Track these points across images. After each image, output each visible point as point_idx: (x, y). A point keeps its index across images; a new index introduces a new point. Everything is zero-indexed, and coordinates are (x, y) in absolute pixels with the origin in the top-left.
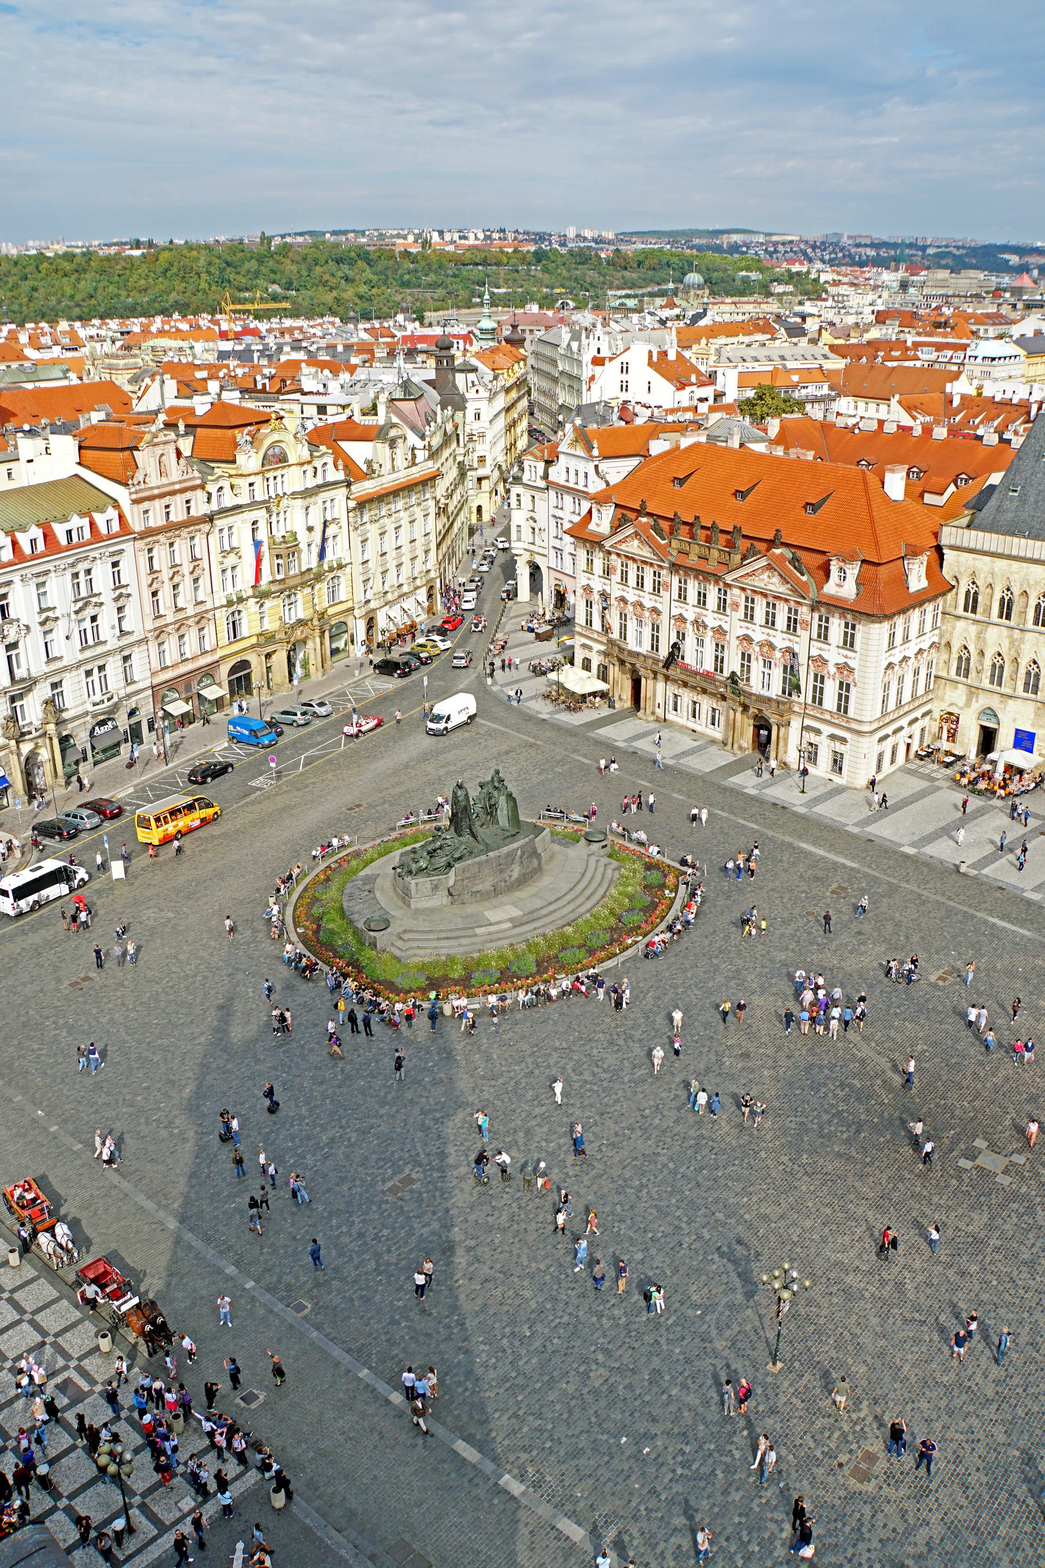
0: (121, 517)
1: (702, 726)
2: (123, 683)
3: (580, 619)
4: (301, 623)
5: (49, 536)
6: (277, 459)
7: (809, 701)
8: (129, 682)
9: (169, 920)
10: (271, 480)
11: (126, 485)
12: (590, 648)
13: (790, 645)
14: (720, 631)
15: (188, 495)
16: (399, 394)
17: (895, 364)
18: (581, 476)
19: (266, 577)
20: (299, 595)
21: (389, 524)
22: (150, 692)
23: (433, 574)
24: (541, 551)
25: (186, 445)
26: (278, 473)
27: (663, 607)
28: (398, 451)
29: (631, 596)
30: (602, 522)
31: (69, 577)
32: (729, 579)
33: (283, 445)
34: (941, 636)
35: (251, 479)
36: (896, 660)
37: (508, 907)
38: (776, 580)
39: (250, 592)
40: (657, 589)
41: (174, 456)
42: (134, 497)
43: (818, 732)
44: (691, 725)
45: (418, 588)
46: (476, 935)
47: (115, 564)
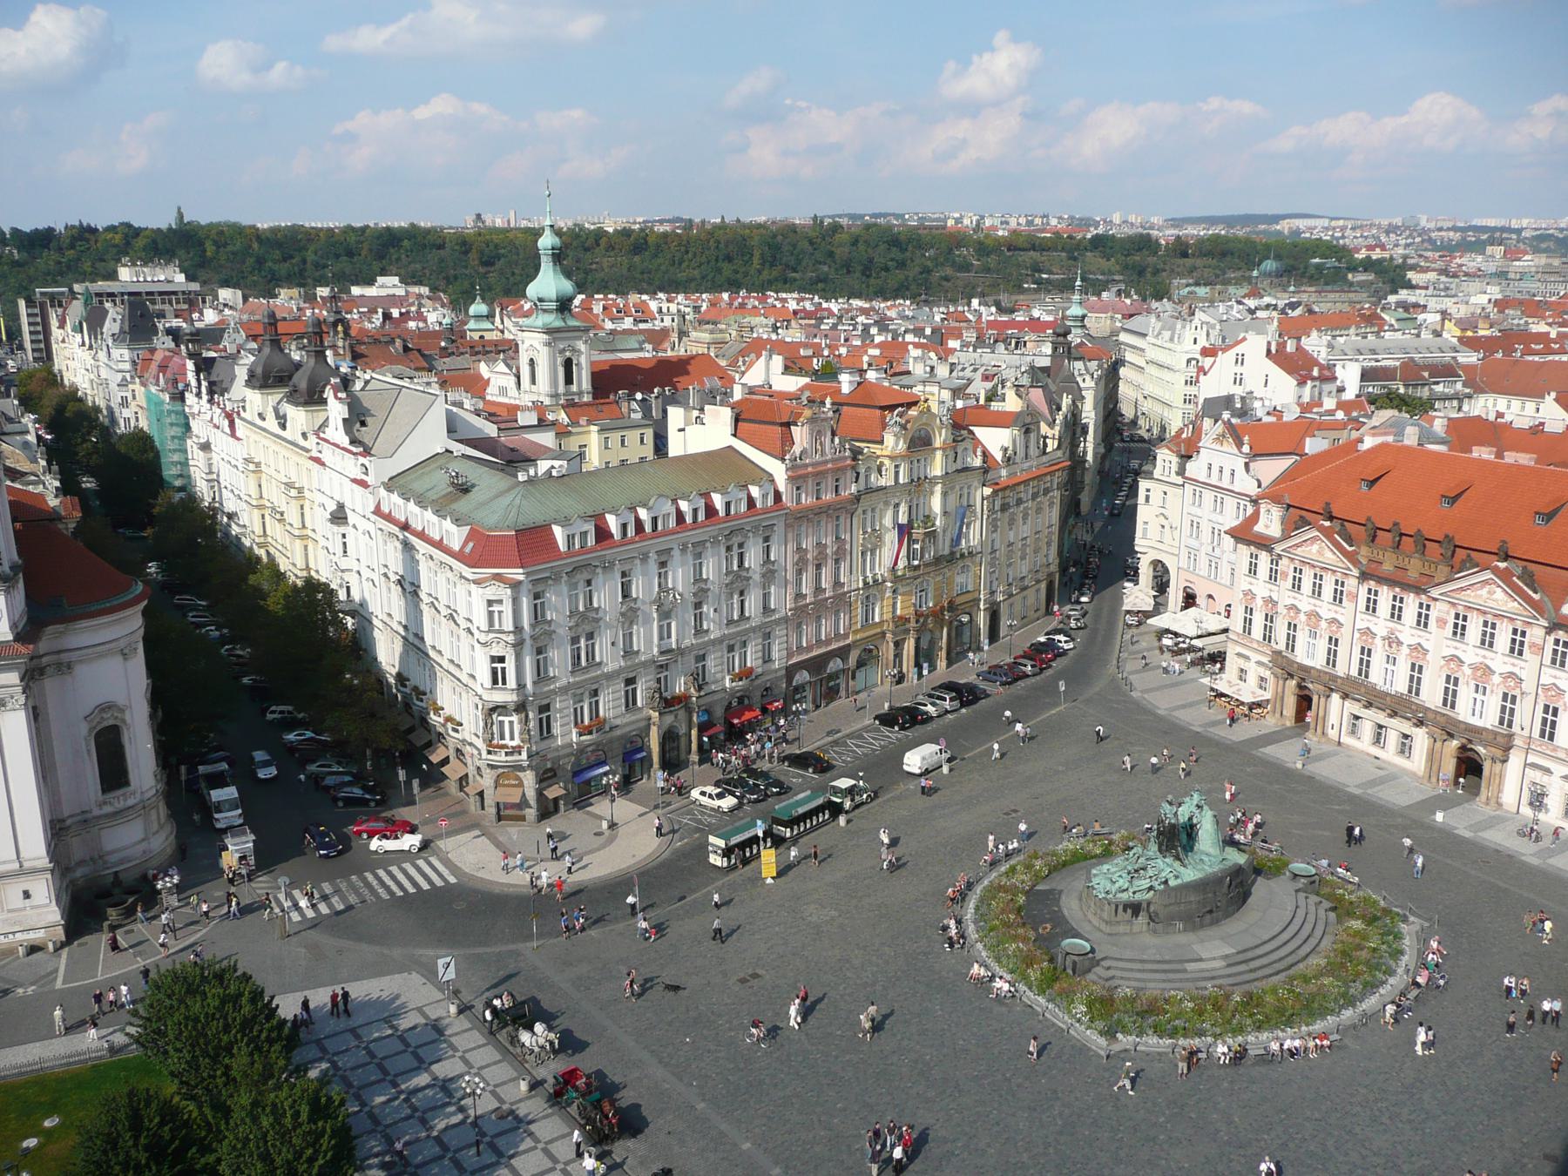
1: (1389, 753)
7: (1536, 733)
9: (833, 919)
11: (783, 460)
12: (1247, 658)
14: (1418, 649)
16: (1025, 381)
17: (1537, 358)
18: (1226, 473)
19: (901, 564)
28: (1033, 436)
29: (1305, 603)
30: (1270, 522)
31: (723, 550)
32: (1435, 593)
37: (1217, 942)
38: (1499, 594)
40: (1338, 598)
44: (1375, 751)
45: (1038, 581)
46: (1185, 971)
47: (766, 539)
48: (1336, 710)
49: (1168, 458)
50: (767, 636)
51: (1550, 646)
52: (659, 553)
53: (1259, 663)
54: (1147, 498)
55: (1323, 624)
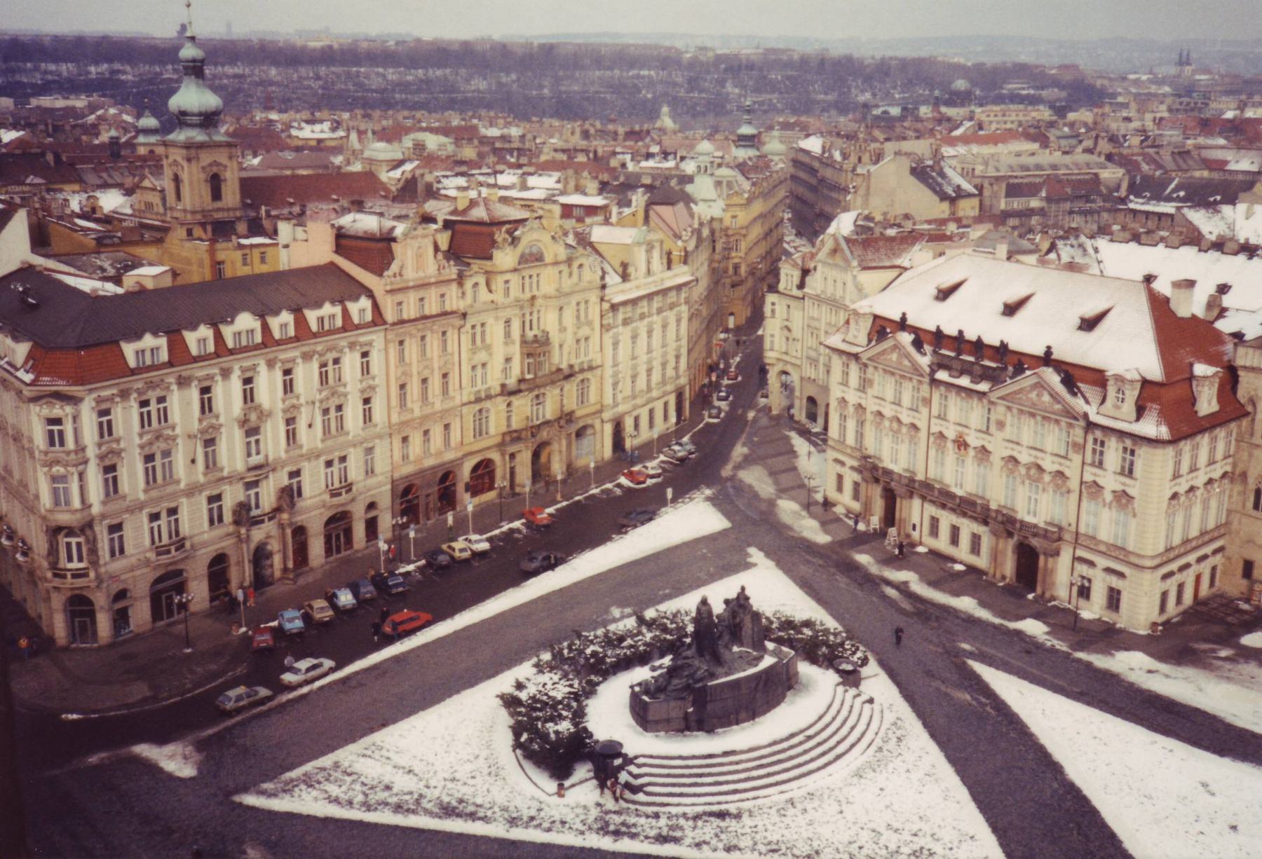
0: (376, 307)
2: (362, 477)
3: (834, 432)
4: (547, 423)
5: (301, 322)
6: (533, 258)
8: (370, 472)
10: (527, 279)
12: (842, 463)
13: (1061, 469)
15: (443, 289)
18: (839, 284)
20: (548, 395)
21: (642, 327)
22: (389, 487)
23: (683, 381)
24: (793, 361)
25: (444, 240)
26: (534, 272)
27: (922, 425)
28: (656, 254)
33: (540, 245)
34: (1235, 465)
35: (508, 276)
36: (1182, 487)
38: (1046, 398)
39: (498, 390)
41: (431, 250)
42: (388, 288)
43: (1091, 564)
45: (665, 394)
47: (365, 355)
48: (915, 512)
49: (790, 272)
50: (370, 451)
51: (1090, 446)
52: (243, 370)
53: (852, 468)
54: (773, 311)
55: (904, 430)
